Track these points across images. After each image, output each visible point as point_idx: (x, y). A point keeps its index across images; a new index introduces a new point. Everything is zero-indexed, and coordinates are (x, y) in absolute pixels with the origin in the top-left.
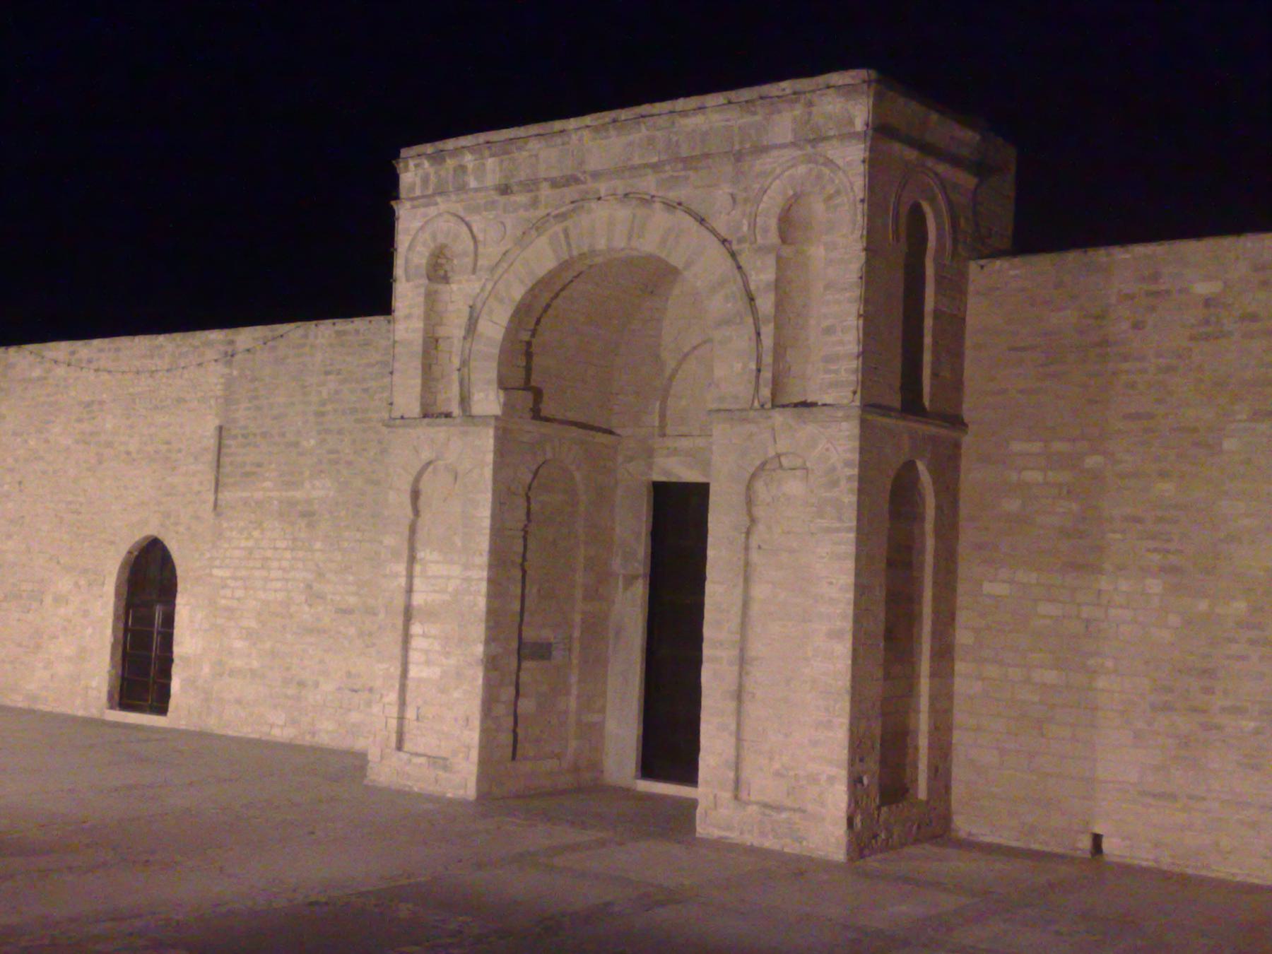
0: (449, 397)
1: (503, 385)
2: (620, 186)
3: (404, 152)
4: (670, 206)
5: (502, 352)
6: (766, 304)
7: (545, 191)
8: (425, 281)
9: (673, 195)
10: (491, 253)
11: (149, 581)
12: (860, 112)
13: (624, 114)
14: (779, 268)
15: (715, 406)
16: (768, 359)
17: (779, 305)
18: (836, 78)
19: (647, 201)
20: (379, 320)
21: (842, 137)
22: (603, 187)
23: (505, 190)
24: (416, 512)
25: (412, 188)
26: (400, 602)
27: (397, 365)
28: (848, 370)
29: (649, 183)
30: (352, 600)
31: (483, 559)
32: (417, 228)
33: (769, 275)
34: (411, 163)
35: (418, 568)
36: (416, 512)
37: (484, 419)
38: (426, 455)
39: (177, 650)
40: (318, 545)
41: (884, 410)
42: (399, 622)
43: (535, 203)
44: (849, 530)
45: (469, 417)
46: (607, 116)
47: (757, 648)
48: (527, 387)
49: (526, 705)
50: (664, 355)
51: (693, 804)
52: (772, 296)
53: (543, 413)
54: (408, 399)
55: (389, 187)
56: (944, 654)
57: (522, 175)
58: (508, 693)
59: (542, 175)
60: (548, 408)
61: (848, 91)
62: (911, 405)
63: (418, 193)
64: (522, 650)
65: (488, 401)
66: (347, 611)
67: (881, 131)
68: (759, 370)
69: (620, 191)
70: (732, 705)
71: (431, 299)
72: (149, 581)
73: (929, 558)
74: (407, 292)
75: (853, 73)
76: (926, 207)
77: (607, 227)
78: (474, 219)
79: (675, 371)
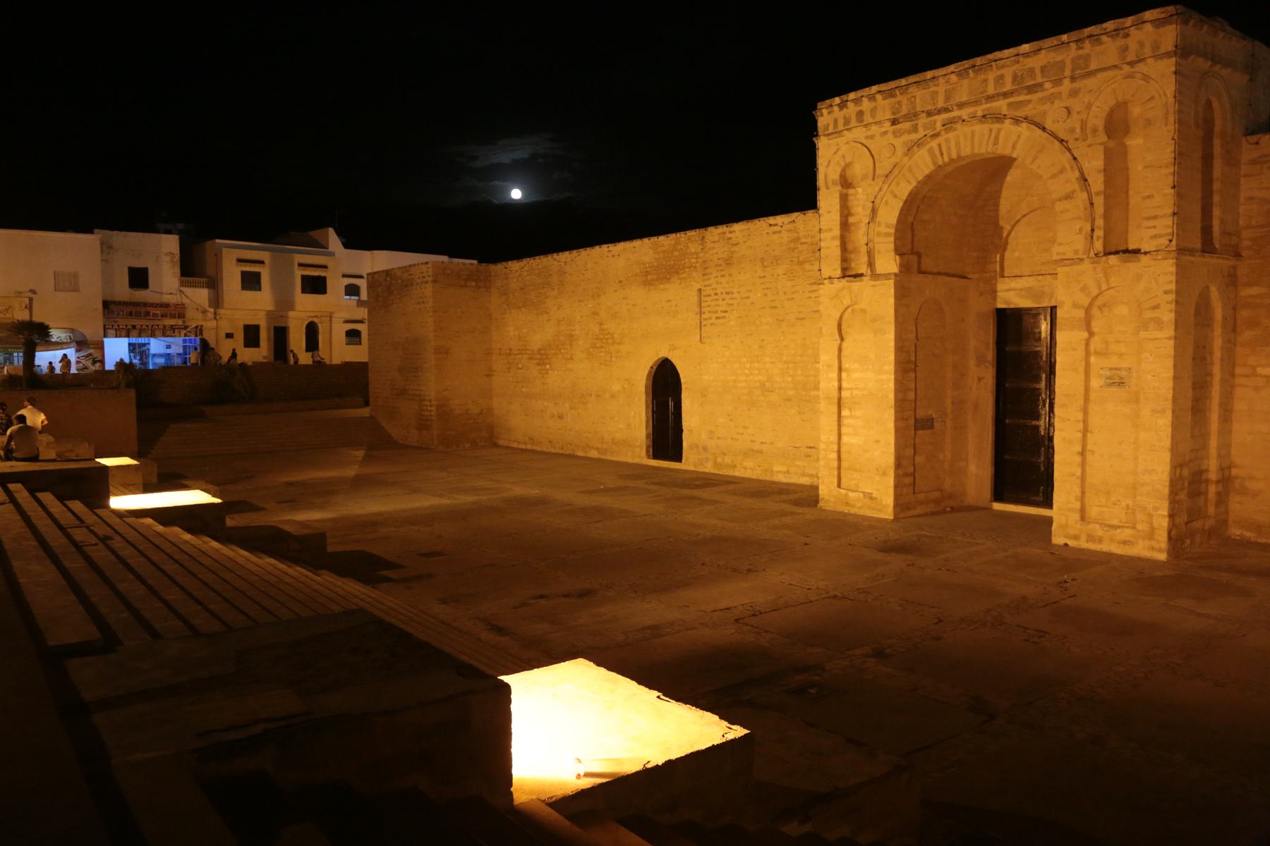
0: (861, 265)
1: (898, 251)
2: (979, 111)
3: (820, 105)
4: (1017, 121)
5: (896, 230)
6: (1097, 182)
7: (923, 120)
8: (839, 188)
9: (1020, 113)
10: (884, 166)
11: (665, 382)
12: (1169, 36)
13: (979, 61)
14: (1106, 158)
15: (1058, 257)
16: (1100, 222)
17: (1108, 182)
18: (1149, 15)
19: (999, 118)
20: (810, 214)
21: (1157, 57)
22: (964, 113)
23: (894, 122)
24: (842, 339)
25: (827, 128)
26: (835, 394)
27: (823, 244)
28: (1166, 225)
29: (1002, 105)
30: (791, 393)
31: (890, 367)
32: (831, 154)
33: (1099, 163)
34: (825, 111)
35: (844, 375)
36: (842, 339)
37: (886, 276)
38: (847, 302)
39: (685, 424)
40: (767, 359)
41: (1191, 252)
42: (835, 409)
43: (915, 129)
44: (1169, 338)
45: (875, 276)
46: (967, 64)
47: (1094, 421)
48: (912, 252)
49: (919, 459)
50: (1002, 223)
51: (1049, 521)
52: (1101, 178)
53: (923, 269)
54: (832, 267)
55: (810, 129)
56: (1227, 415)
57: (904, 111)
58: (910, 452)
59: (919, 108)
60: (927, 263)
61: (1158, 23)
62: (1208, 247)
63: (831, 130)
64: (916, 422)
65: (888, 263)
66: (788, 400)
67: (1183, 51)
68: (1093, 230)
69: (980, 113)
70: (1078, 459)
71: (844, 199)
72: (665, 382)
73: (1217, 354)
74: (828, 198)
75: (1158, 10)
76: (1216, 105)
77: (971, 140)
78: (869, 146)
79: (1009, 234)
